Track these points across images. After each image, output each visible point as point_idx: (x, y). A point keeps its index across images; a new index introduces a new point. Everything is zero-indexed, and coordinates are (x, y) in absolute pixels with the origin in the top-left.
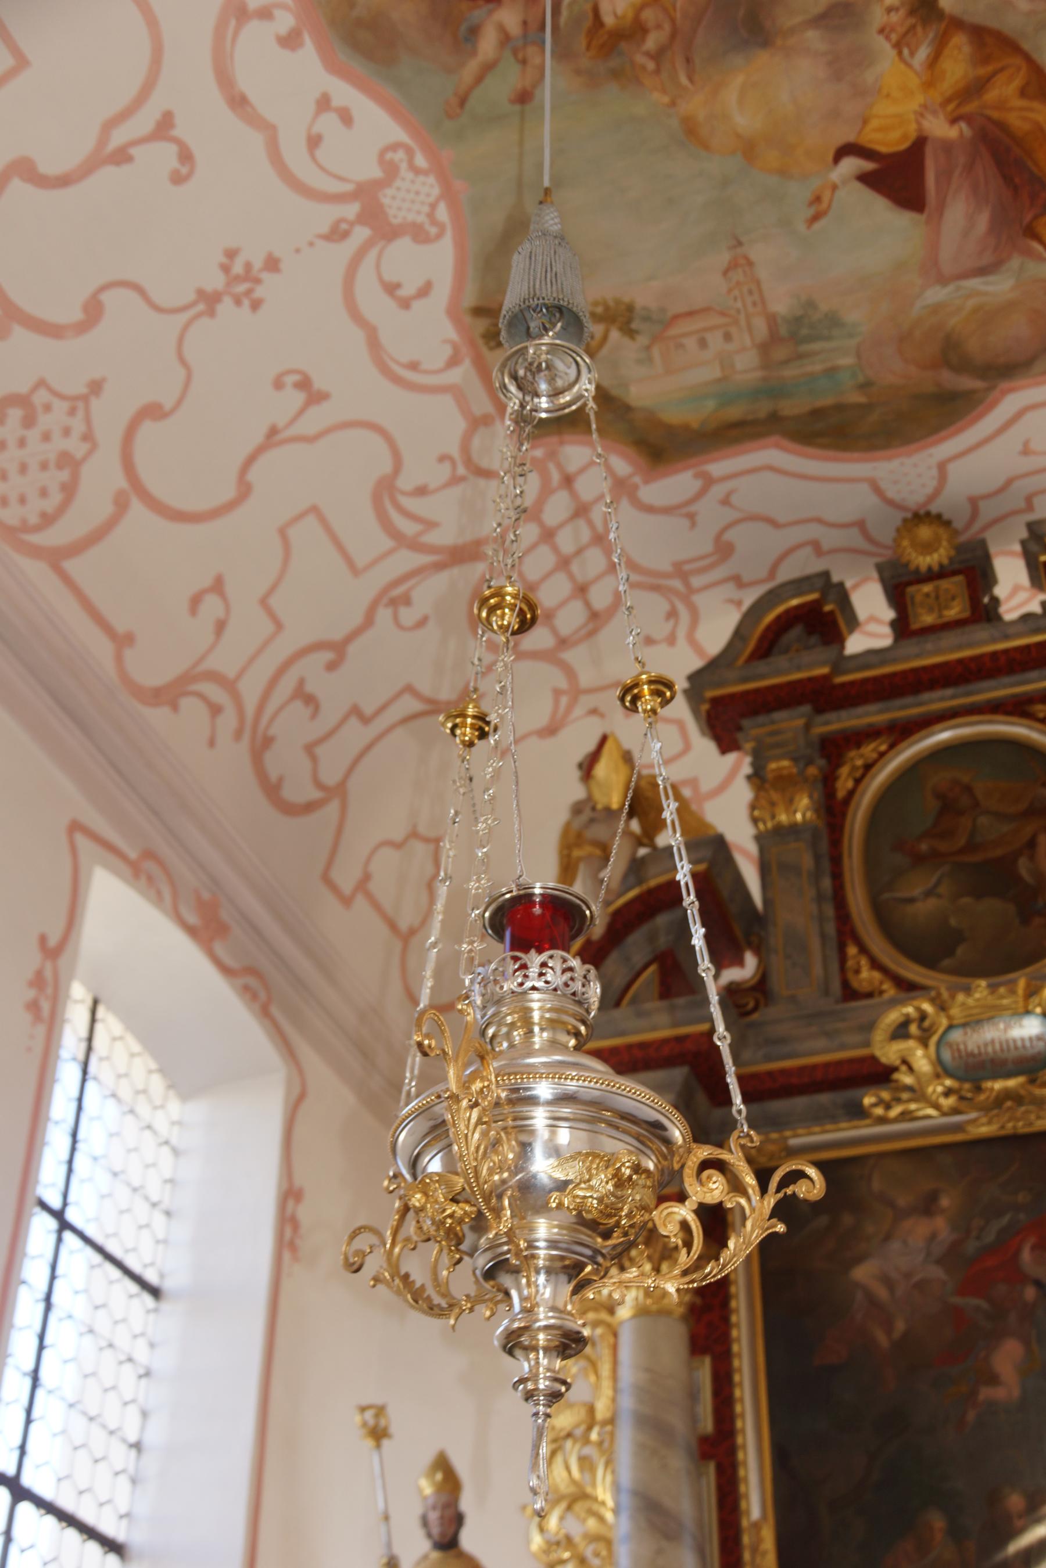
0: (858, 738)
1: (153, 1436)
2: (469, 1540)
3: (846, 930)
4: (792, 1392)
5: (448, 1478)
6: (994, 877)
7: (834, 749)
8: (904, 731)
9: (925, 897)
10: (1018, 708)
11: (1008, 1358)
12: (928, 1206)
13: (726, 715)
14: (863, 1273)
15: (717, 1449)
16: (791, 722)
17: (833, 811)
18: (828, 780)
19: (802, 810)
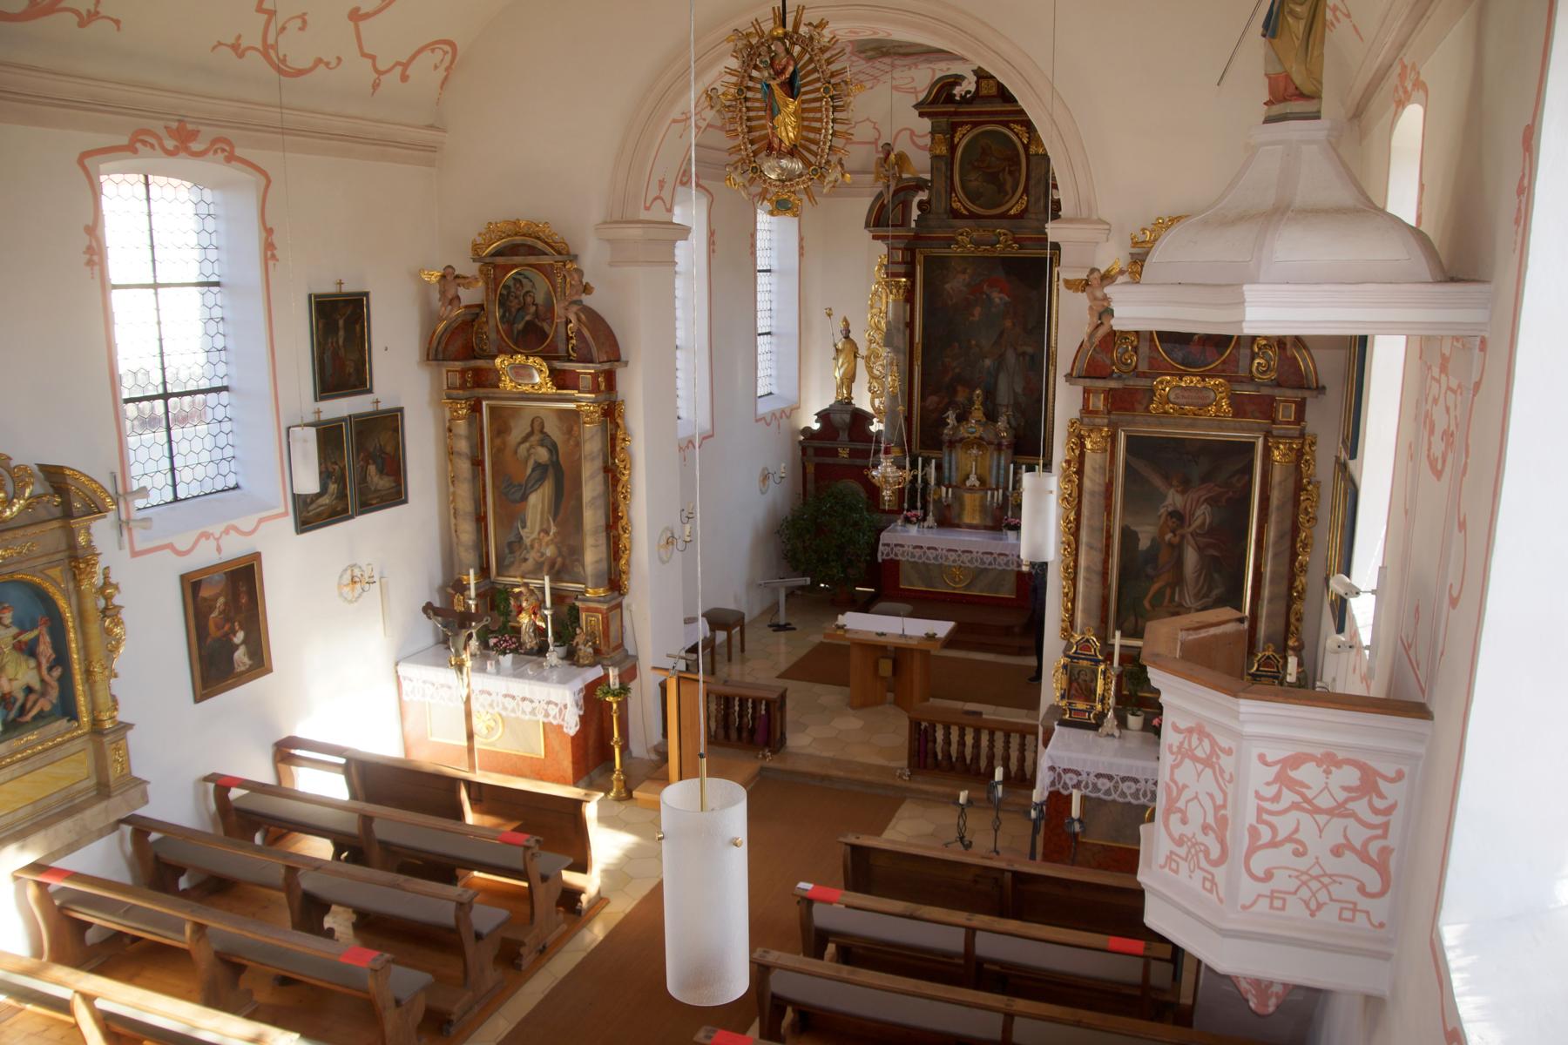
0: (962, 124)
1: (774, 306)
2: (851, 336)
3: (953, 189)
4: (927, 313)
5: (845, 320)
6: (993, 177)
7: (954, 127)
8: (975, 125)
9: (975, 181)
10: (1006, 124)
11: (977, 311)
12: (964, 272)
13: (923, 109)
14: (947, 286)
15: (910, 325)
16: (944, 120)
17: (953, 148)
18: (952, 137)
19: (943, 150)
